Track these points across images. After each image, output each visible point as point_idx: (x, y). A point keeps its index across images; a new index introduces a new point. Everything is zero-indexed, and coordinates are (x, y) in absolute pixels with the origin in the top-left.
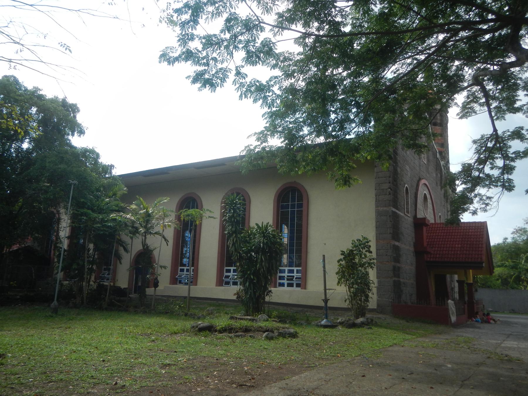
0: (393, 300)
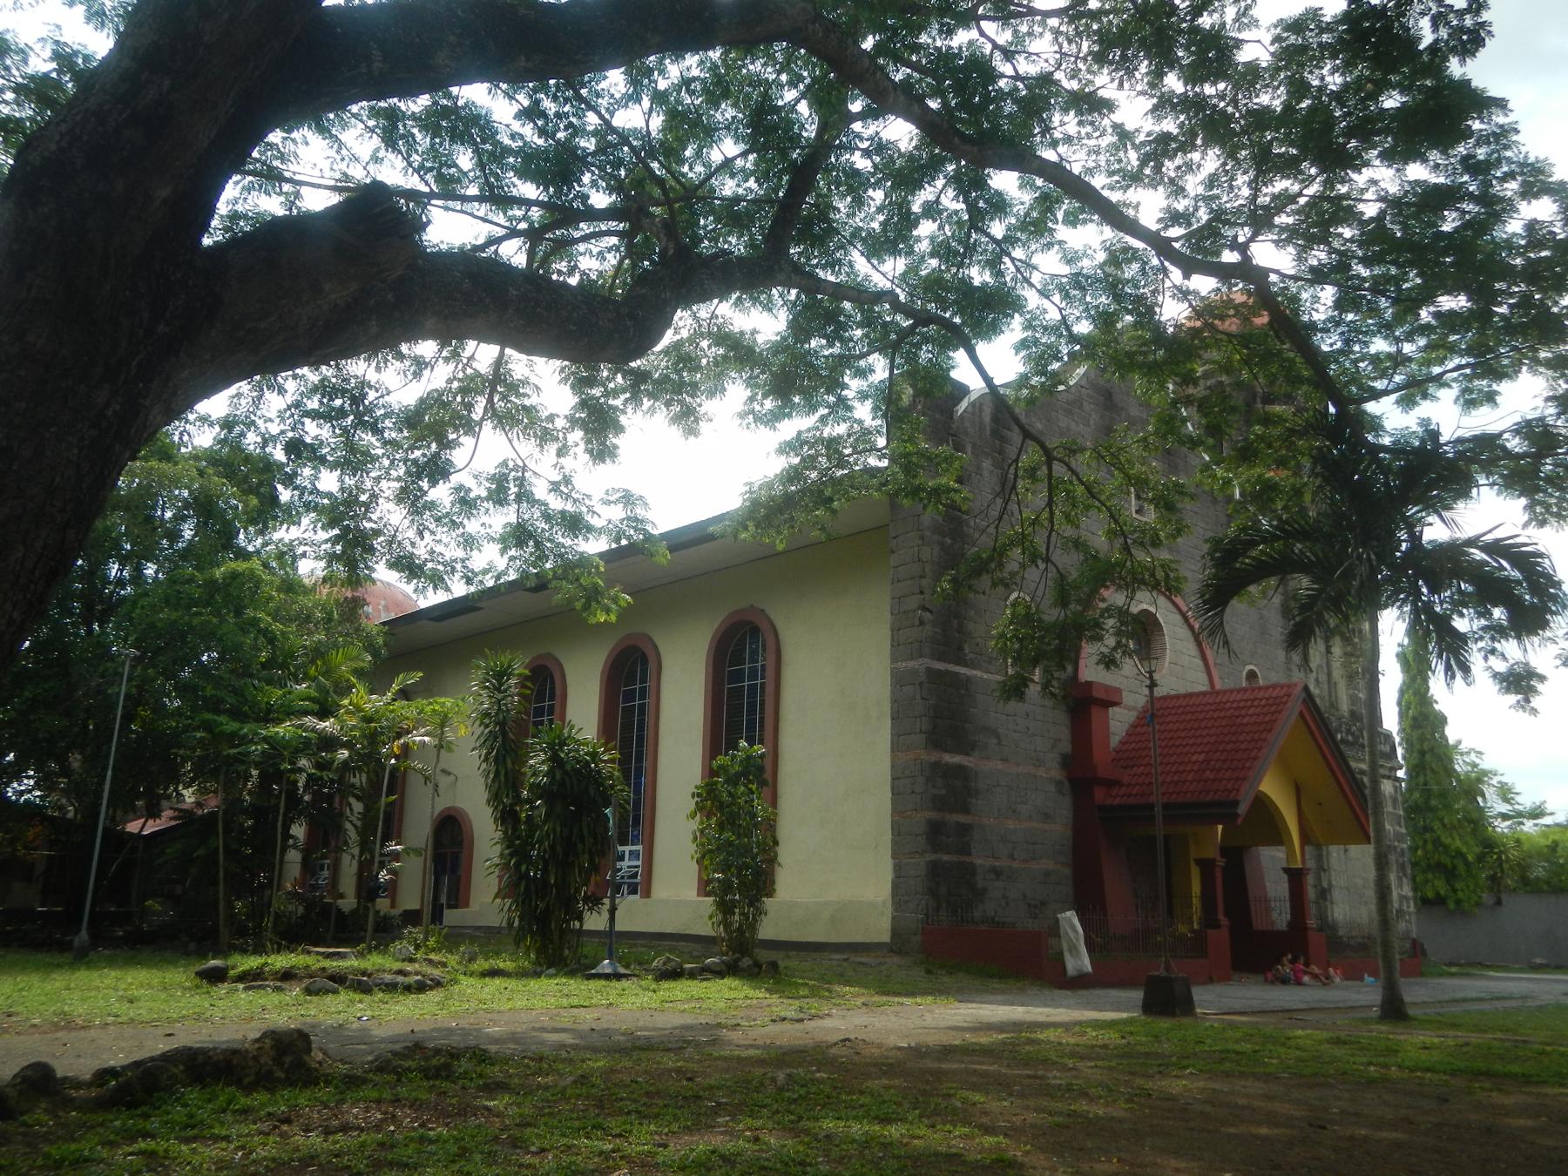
0: (927, 915)
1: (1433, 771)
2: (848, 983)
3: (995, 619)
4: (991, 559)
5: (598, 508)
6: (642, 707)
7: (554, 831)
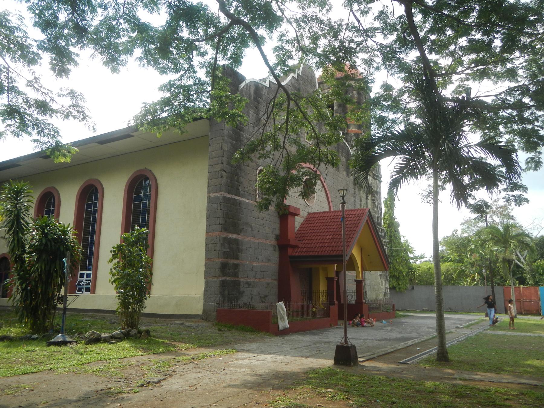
0: (219, 304)
1: (394, 243)
2: (183, 341)
3: (257, 172)
4: (259, 145)
5: (56, 98)
6: (95, 211)
7: (41, 267)
